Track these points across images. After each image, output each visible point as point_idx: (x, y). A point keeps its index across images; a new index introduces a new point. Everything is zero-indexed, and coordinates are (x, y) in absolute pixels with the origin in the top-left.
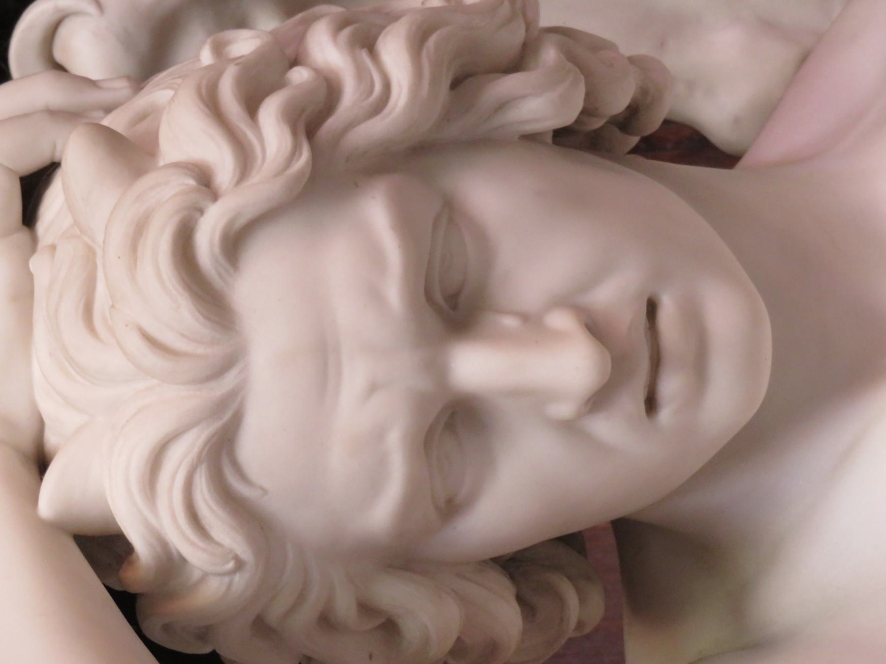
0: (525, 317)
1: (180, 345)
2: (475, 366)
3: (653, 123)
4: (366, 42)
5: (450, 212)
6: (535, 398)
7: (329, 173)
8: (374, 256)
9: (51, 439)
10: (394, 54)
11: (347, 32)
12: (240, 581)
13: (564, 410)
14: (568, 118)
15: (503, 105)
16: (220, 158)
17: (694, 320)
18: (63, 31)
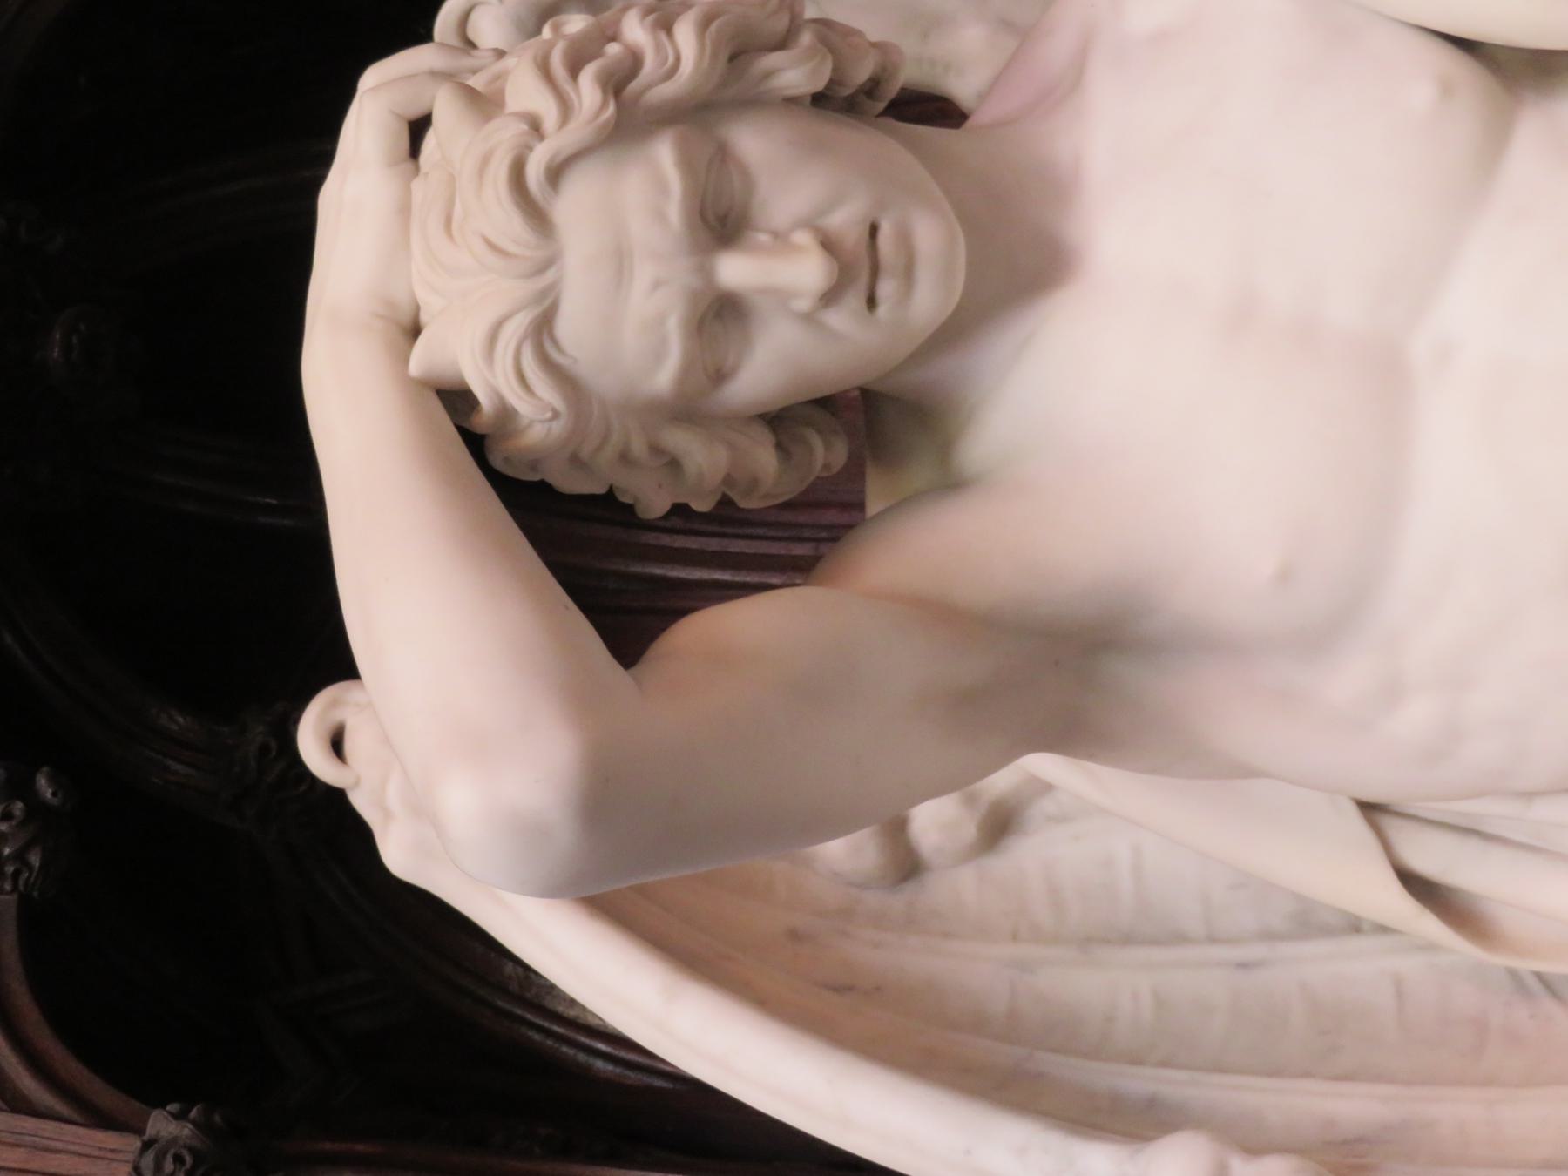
0: (776, 235)
1: (512, 248)
2: (735, 270)
3: (892, 91)
4: (665, 26)
5: (723, 154)
6: (781, 296)
7: (629, 122)
8: (662, 187)
9: (424, 317)
10: (685, 33)
11: (651, 18)
12: (558, 428)
13: (803, 305)
14: (819, 85)
15: (768, 75)
16: (546, 107)
18: (474, 16)
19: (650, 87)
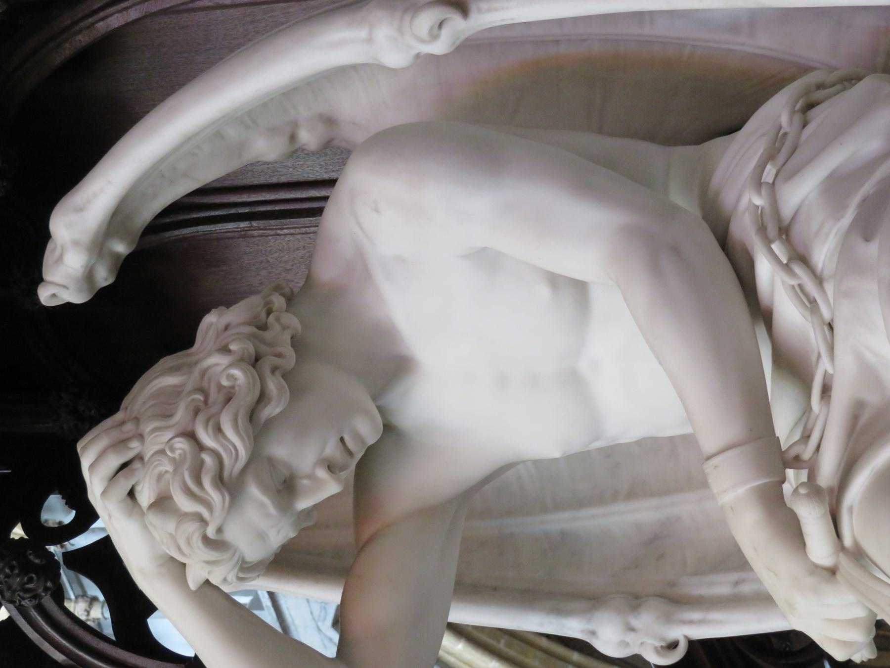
2: (303, 504)
4: (218, 430)
5: (271, 462)
8: (263, 505)
17: (357, 437)
19: (233, 468)
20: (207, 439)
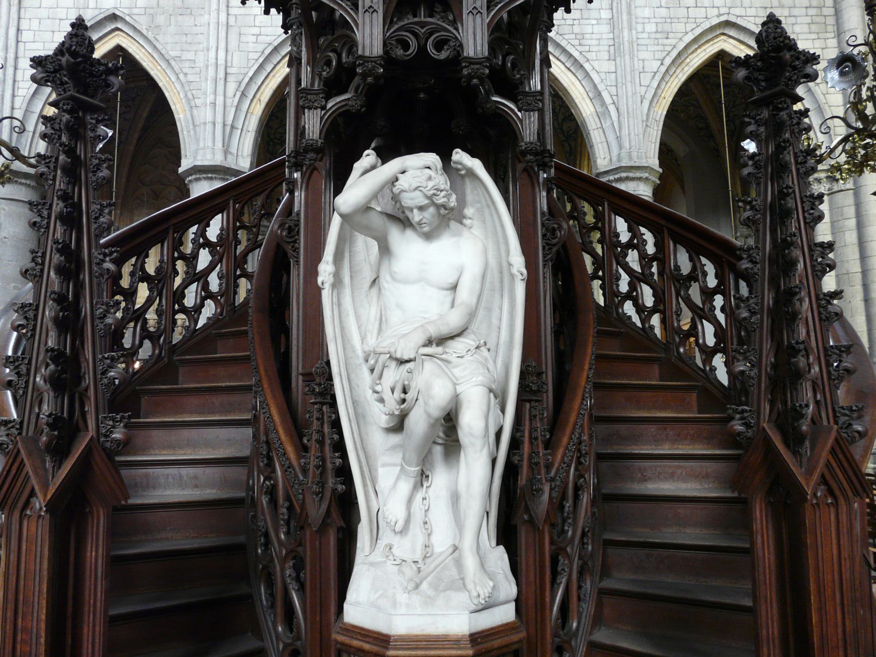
2: (415, 211)
7: (429, 198)
20: (443, 193)
